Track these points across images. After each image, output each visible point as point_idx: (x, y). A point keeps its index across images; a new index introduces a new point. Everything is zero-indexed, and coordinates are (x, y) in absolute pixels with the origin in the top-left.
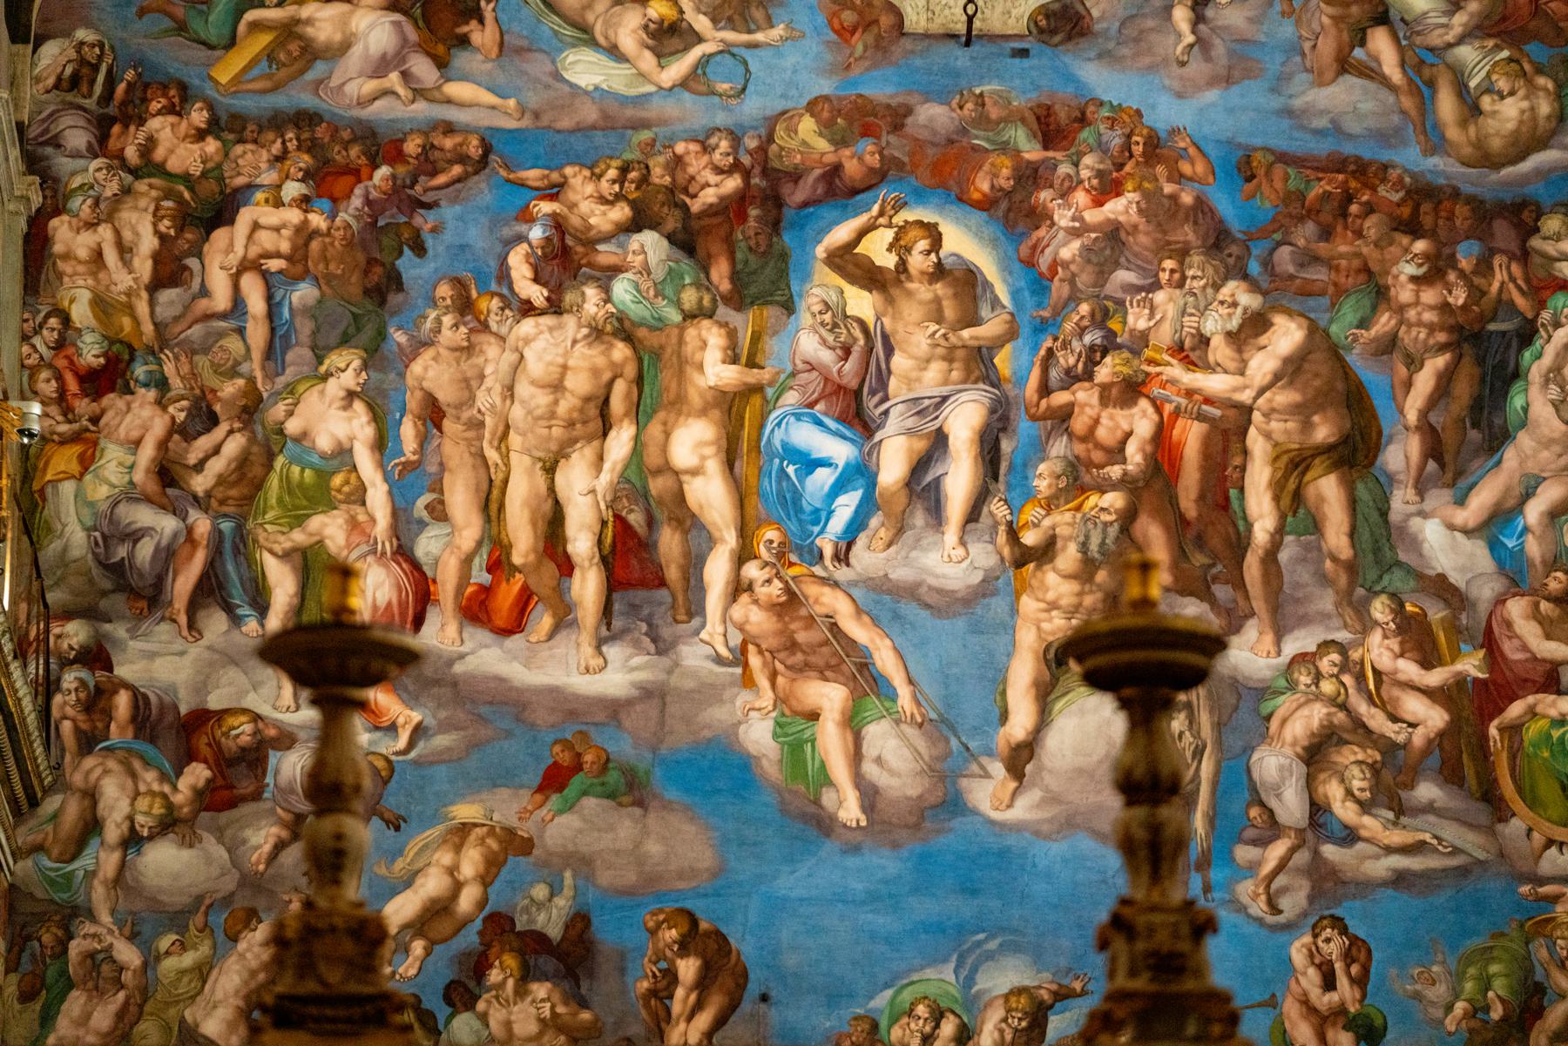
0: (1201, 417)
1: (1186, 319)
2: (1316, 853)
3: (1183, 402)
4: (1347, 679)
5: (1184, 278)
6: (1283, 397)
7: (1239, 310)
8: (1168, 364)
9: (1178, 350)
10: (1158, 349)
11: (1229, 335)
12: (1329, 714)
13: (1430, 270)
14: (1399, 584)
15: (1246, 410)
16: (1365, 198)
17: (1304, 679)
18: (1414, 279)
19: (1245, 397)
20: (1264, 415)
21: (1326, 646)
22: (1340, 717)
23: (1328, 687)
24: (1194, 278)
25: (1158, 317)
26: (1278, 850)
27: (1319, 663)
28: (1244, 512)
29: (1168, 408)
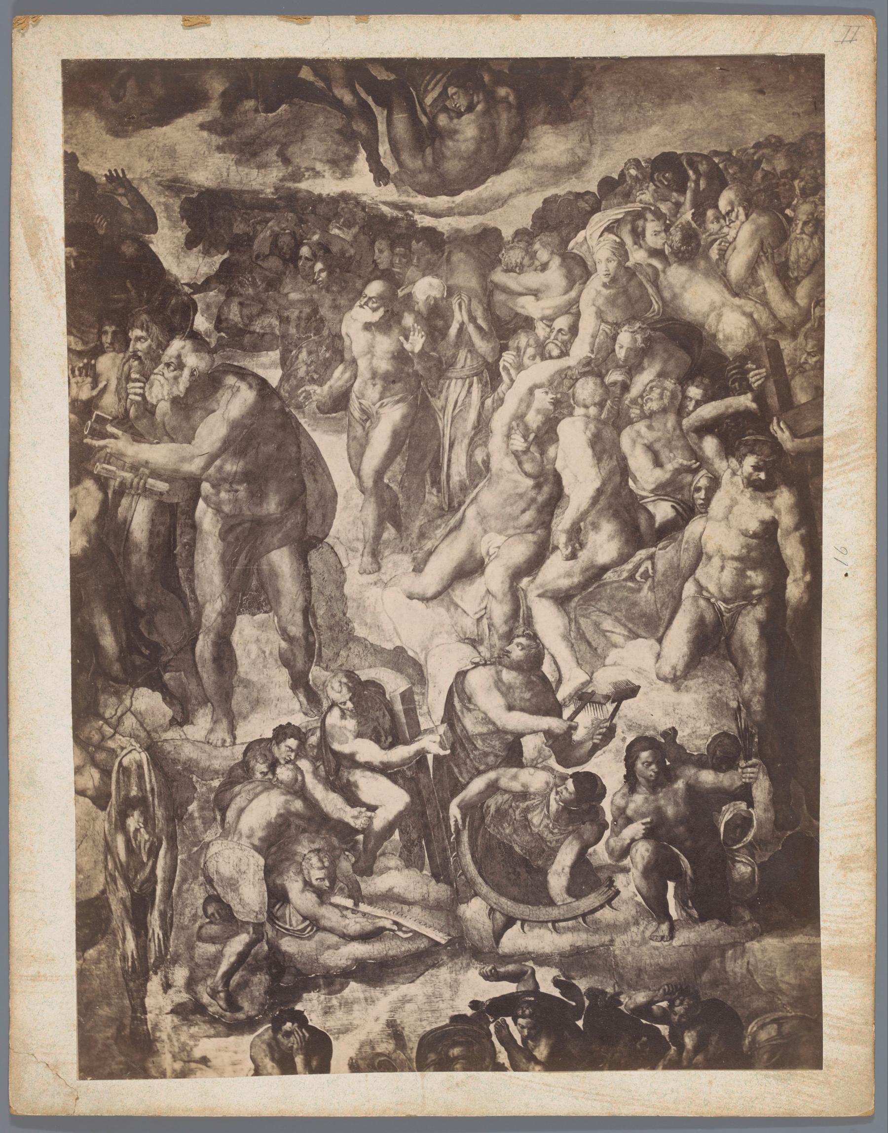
0: (147, 492)
1: (131, 385)
2: (274, 949)
3: (128, 476)
4: (304, 765)
5: (127, 341)
6: (231, 467)
7: (186, 373)
8: (116, 437)
9: (123, 421)
10: (101, 420)
11: (175, 401)
12: (287, 802)
13: (386, 312)
14: (356, 661)
15: (193, 484)
16: (316, 237)
17: (261, 767)
18: (368, 326)
19: (194, 467)
20: (213, 486)
21: (282, 732)
22: (298, 805)
23: (284, 773)
24: (138, 339)
25: (101, 385)
26: (238, 944)
27: (275, 749)
28: (193, 591)
29: (114, 484)
